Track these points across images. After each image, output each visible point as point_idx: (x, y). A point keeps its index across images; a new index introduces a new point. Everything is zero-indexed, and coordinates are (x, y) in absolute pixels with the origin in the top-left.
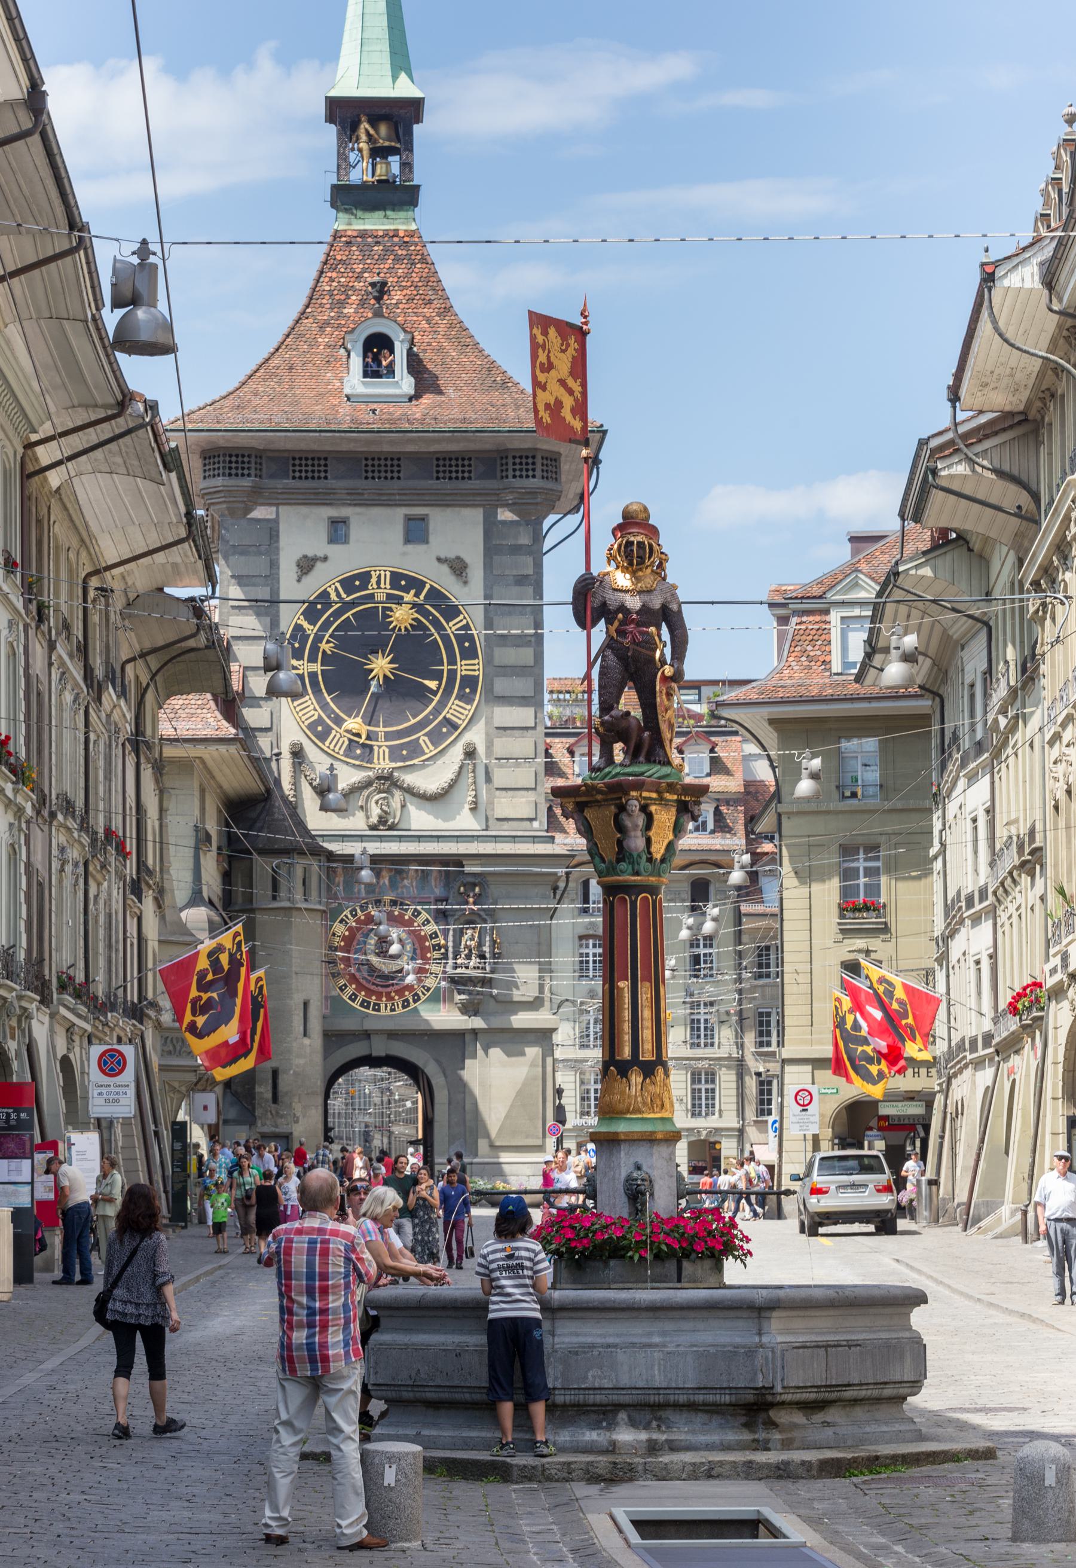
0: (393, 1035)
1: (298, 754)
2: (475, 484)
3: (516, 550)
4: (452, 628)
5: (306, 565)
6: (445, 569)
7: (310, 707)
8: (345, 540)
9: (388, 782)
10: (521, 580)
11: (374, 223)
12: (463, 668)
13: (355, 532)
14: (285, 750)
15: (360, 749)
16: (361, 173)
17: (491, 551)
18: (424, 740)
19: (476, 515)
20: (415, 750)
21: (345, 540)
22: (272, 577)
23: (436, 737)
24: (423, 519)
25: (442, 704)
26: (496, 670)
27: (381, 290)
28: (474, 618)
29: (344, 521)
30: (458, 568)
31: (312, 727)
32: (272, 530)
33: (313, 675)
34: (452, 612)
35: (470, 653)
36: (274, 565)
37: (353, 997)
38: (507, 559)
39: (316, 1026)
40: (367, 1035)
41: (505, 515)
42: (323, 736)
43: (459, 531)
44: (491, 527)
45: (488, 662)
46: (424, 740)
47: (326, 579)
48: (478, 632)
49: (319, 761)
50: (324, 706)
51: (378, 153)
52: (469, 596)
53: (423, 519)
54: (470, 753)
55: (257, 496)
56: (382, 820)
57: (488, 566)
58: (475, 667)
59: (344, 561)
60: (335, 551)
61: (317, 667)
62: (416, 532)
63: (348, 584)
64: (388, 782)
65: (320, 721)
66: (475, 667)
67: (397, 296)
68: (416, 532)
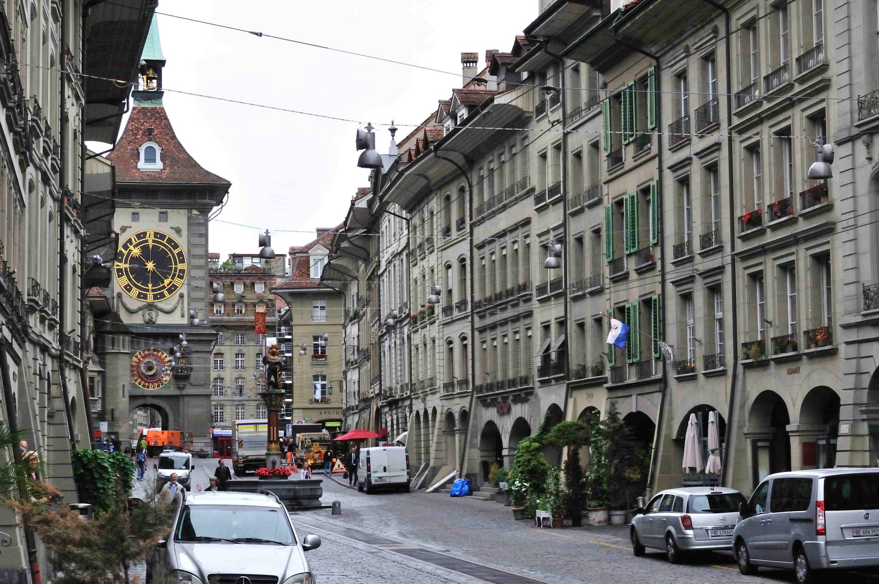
0: (154, 397)
1: (119, 296)
2: (184, 201)
3: (199, 224)
4: (176, 252)
6: (173, 231)
8: (138, 220)
9: (151, 307)
10: (201, 235)
12: (180, 266)
13: (141, 217)
14: (115, 295)
17: (190, 225)
18: (166, 292)
19: (184, 212)
20: (162, 296)
21: (138, 220)
23: (170, 291)
24: (166, 213)
25: (173, 278)
26: (192, 267)
28: (183, 247)
29: (137, 214)
30: (178, 231)
31: (125, 287)
33: (126, 269)
34: (176, 246)
35: (182, 261)
37: (140, 384)
38: (195, 228)
40: (144, 397)
41: (195, 212)
42: (129, 291)
43: (178, 218)
45: (189, 264)
46: (166, 292)
48: (185, 253)
49: (126, 299)
52: (182, 242)
53: (166, 213)
54: (182, 296)
57: (189, 230)
60: (133, 224)
62: (163, 217)
63: (138, 236)
64: (151, 307)
65: (128, 285)
67: (156, 131)
68: (163, 217)
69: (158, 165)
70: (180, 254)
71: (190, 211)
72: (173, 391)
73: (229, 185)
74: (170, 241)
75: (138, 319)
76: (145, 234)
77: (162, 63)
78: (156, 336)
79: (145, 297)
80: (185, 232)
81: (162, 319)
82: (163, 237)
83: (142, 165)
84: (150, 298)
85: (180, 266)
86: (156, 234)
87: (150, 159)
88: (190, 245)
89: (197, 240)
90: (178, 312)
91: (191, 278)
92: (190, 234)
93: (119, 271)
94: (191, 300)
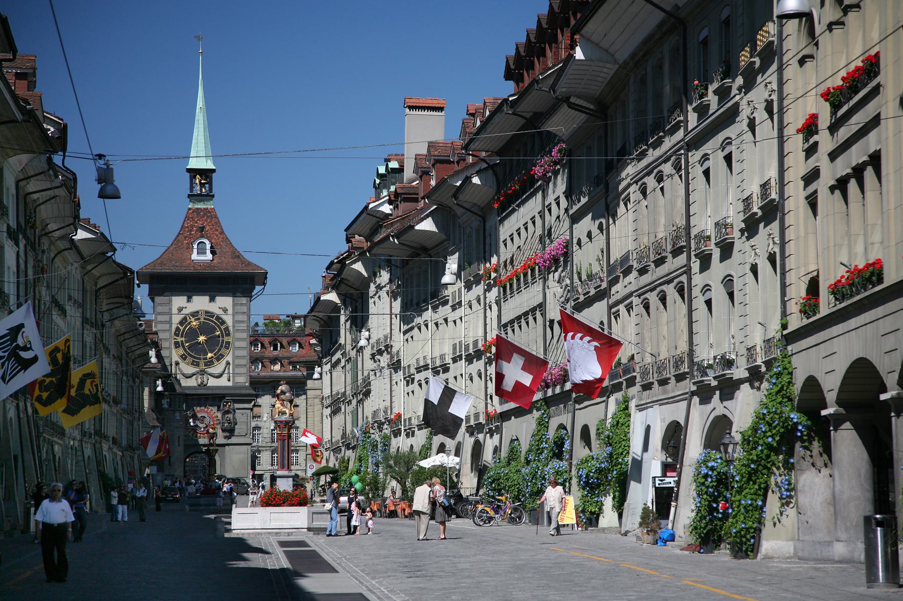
7: (181, 351)
22: (170, 314)
23: (218, 359)
25: (220, 350)
31: (181, 356)
34: (223, 322)
36: (171, 309)
39: (182, 443)
42: (185, 359)
48: (231, 329)
50: (185, 350)
54: (228, 363)
56: (202, 383)
57: (233, 309)
61: (183, 339)
64: (203, 372)
68: (212, 300)
69: (209, 256)
70: (227, 329)
74: (218, 318)
75: (192, 383)
76: (198, 312)
80: (230, 311)
81: (212, 382)
83: (195, 256)
86: (206, 312)
88: (235, 322)
90: (225, 376)
94: (236, 366)
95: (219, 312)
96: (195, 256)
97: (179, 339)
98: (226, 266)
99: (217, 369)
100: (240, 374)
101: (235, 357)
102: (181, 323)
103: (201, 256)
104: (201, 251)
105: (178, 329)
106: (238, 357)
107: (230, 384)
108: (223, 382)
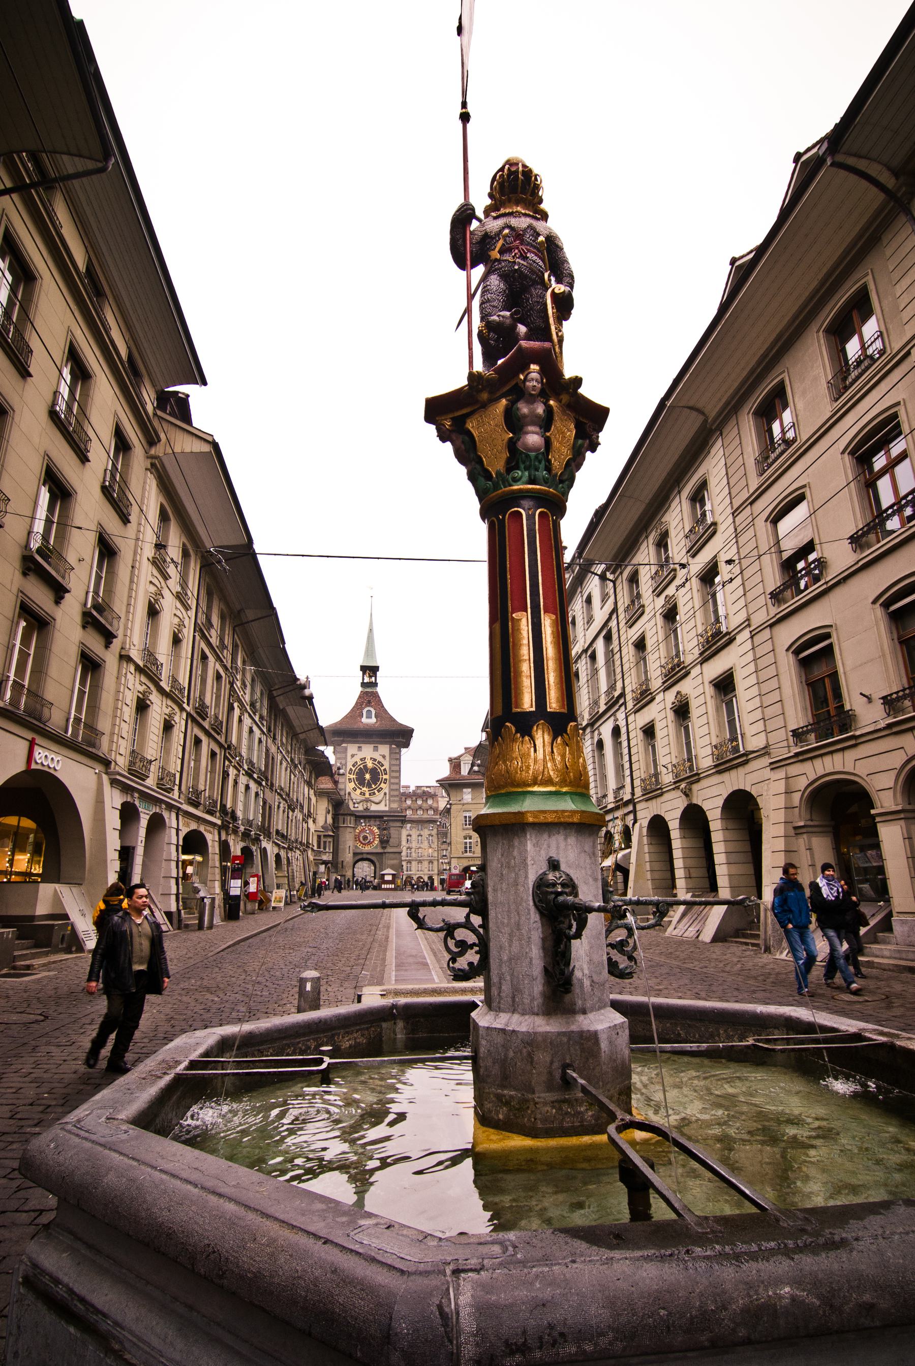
0: (368, 853)
1: (349, 794)
5: (353, 756)
7: (352, 785)
9: (367, 800)
10: (397, 759)
11: (369, 690)
12: (385, 777)
15: (363, 794)
16: (367, 680)
17: (391, 753)
20: (374, 794)
22: (346, 758)
23: (379, 791)
26: (391, 777)
27: (369, 702)
30: (384, 757)
32: (346, 749)
34: (382, 765)
39: (351, 852)
40: (362, 853)
43: (384, 749)
44: (391, 749)
47: (357, 759)
49: (353, 795)
51: (370, 677)
54: (385, 794)
55: (343, 742)
58: (387, 777)
59: (361, 755)
62: (376, 749)
63: (361, 760)
64: (367, 800)
66: (387, 777)
68: (376, 749)
69: (373, 720)
70: (385, 770)
71: (391, 745)
72: (379, 850)
73: (412, 730)
74: (379, 762)
77: (378, 667)
78: (370, 817)
79: (364, 794)
81: (374, 807)
82: (375, 760)
83: (364, 720)
84: (367, 795)
85: (385, 777)
87: (369, 716)
88: (391, 765)
89: (394, 762)
90: (383, 803)
91: (391, 783)
92: (391, 759)
93: (350, 779)
94: (391, 796)
95: (380, 759)
96: (364, 720)
97: (352, 776)
98: (386, 726)
99: (378, 797)
100: (394, 801)
101: (391, 790)
102: (354, 766)
103: (369, 720)
104: (369, 716)
105: (351, 769)
106: (392, 790)
107: (387, 809)
108: (382, 807)
